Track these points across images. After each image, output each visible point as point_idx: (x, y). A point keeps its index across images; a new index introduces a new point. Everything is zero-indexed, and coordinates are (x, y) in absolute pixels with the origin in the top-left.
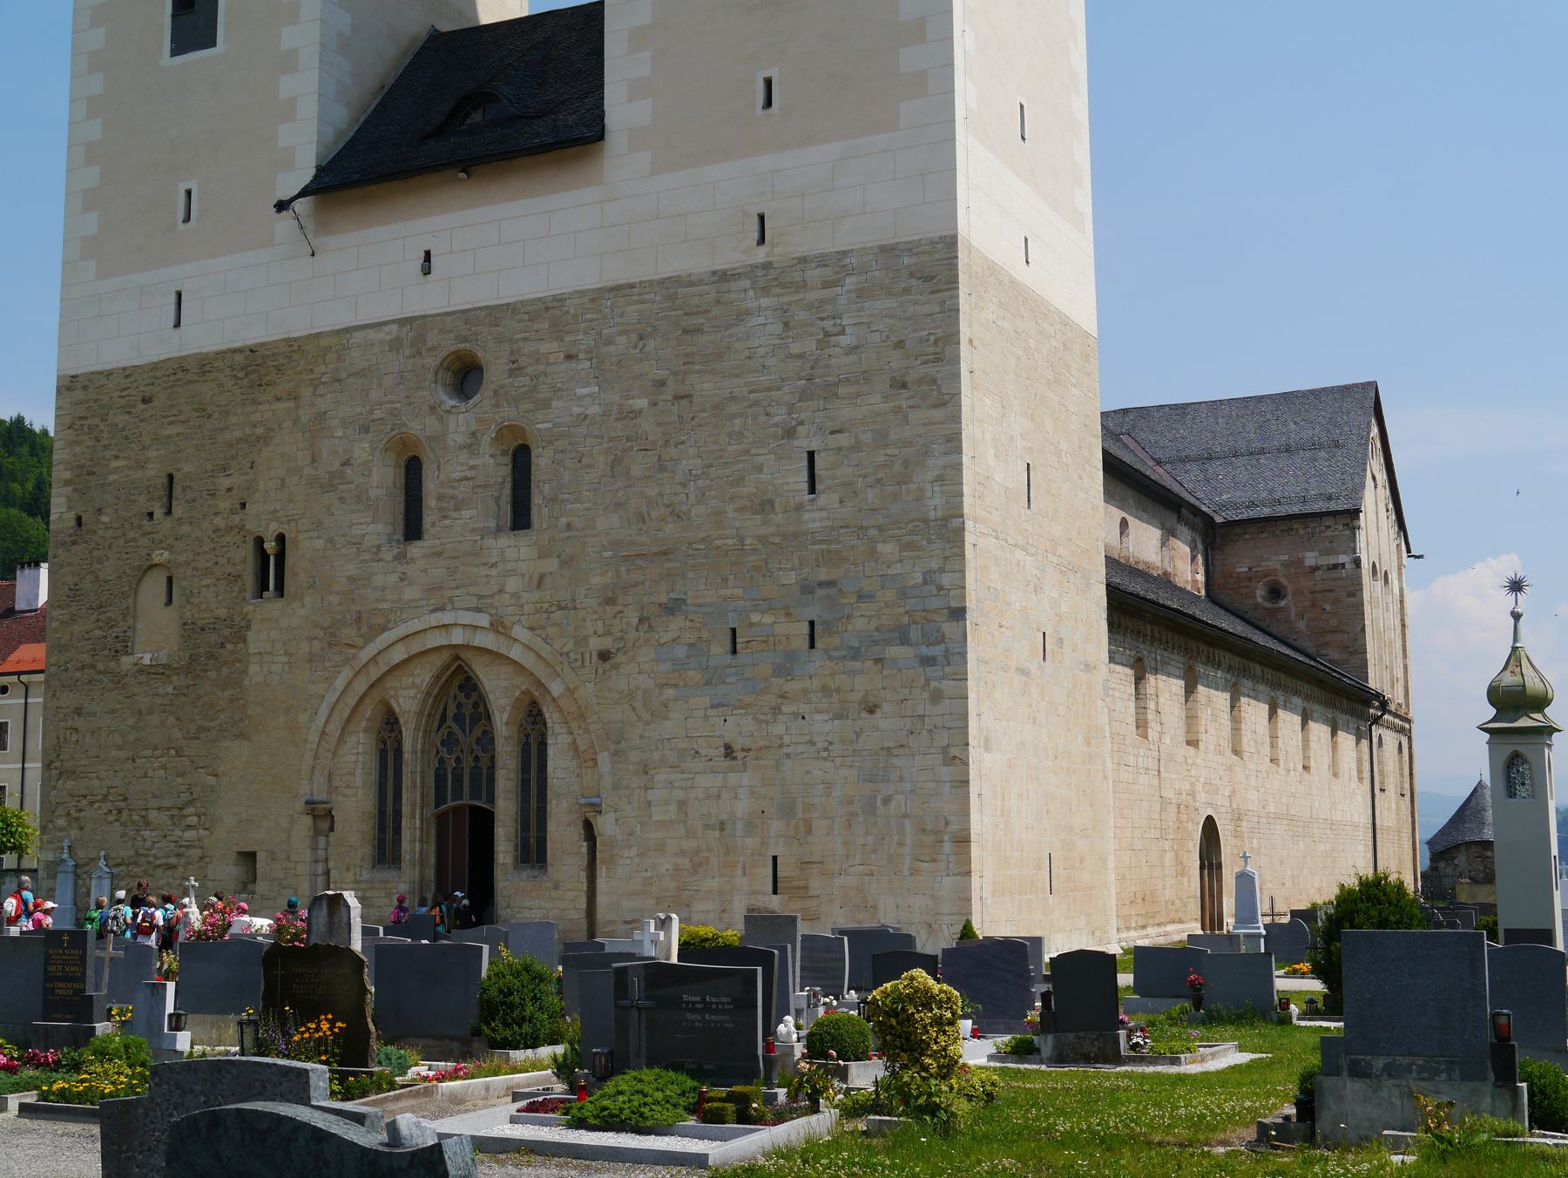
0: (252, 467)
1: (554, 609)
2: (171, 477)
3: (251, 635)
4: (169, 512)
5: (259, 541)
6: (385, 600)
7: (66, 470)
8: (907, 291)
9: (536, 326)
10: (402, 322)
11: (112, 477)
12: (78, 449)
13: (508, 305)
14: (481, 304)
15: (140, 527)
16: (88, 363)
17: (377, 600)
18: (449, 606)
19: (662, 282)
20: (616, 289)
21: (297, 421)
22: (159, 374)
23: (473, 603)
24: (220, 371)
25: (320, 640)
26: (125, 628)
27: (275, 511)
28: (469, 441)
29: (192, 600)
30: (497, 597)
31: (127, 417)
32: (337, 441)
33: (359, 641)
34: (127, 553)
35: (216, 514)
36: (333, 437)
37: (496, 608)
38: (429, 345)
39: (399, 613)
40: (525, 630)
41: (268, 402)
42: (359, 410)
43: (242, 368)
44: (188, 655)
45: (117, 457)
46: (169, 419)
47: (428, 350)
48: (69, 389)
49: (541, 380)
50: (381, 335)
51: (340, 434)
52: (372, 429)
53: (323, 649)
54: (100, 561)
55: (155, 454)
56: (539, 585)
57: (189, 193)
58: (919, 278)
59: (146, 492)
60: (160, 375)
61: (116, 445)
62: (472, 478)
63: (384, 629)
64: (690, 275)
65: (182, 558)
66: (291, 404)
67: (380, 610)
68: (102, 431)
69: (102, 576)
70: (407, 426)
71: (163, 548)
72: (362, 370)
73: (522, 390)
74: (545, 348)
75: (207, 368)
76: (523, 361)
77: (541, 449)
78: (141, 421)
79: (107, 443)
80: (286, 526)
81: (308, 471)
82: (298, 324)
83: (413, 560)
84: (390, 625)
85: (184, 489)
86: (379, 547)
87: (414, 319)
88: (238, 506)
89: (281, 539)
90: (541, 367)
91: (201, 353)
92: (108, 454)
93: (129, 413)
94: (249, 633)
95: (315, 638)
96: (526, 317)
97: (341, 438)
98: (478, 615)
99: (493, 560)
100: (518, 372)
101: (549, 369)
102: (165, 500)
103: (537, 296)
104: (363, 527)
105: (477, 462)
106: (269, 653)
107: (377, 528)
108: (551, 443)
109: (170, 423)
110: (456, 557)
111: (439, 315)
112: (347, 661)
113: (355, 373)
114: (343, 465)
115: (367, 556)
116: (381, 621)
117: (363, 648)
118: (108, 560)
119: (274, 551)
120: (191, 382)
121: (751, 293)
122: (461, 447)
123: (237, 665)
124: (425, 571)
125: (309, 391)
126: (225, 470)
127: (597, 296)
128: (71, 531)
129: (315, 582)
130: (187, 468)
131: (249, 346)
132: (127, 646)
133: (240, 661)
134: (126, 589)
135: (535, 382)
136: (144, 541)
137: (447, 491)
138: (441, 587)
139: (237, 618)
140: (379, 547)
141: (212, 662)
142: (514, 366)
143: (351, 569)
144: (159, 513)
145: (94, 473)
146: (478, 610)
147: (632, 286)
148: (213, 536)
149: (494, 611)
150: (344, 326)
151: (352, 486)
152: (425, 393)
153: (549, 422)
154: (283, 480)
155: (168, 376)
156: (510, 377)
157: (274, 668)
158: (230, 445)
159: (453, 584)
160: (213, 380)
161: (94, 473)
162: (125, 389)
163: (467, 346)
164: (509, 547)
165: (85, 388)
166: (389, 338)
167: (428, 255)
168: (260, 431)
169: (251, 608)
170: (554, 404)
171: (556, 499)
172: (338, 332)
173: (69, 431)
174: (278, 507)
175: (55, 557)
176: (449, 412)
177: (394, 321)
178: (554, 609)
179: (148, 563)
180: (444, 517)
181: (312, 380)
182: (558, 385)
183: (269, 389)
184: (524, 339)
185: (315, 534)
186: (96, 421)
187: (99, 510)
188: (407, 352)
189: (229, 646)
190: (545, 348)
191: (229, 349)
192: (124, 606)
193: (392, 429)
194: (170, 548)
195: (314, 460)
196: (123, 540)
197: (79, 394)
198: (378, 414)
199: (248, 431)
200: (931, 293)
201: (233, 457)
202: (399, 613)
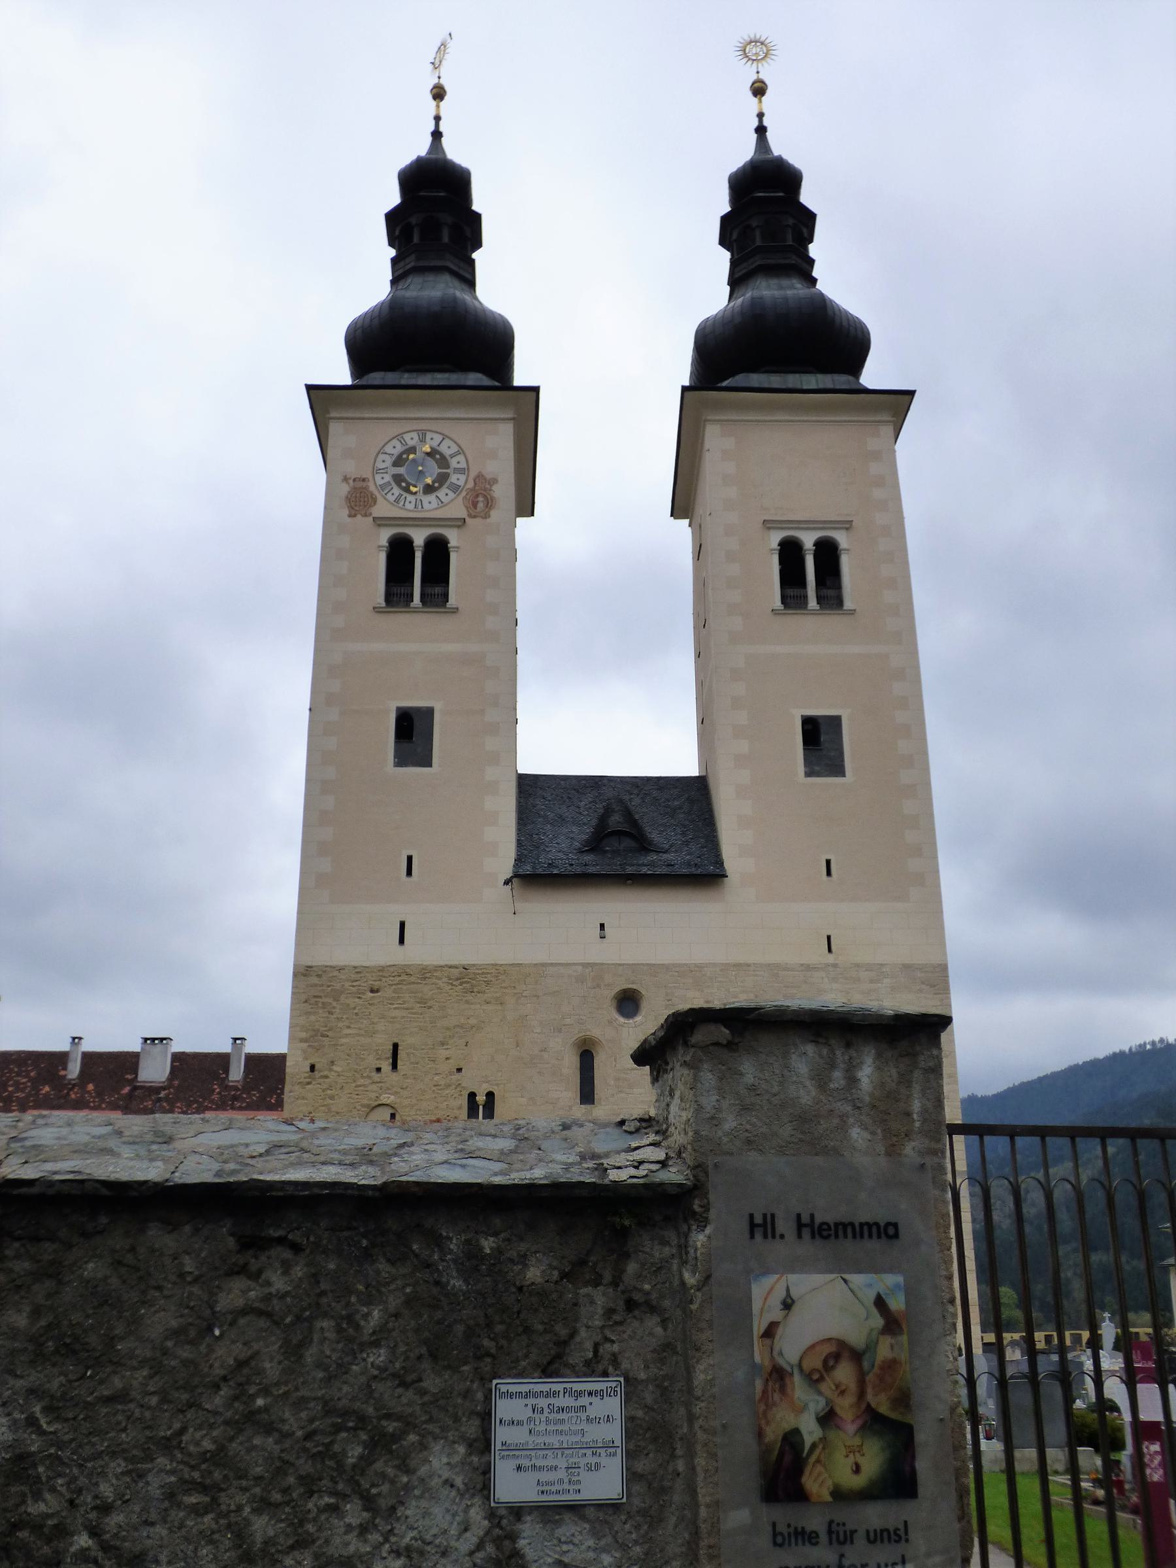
2: (396, 1046)
4: (395, 1066)
5: (472, 1096)
7: (301, 1031)
8: (921, 991)
10: (585, 965)
11: (343, 1041)
12: (313, 1018)
15: (369, 1077)
16: (322, 957)
19: (769, 965)
20: (738, 966)
22: (385, 974)
24: (440, 979)
31: (357, 1000)
41: (479, 1003)
43: (457, 979)
45: (349, 1027)
46: (394, 1006)
47: (605, 986)
48: (305, 975)
51: (538, 1030)
54: (332, 1098)
57: (410, 859)
58: (927, 985)
60: (387, 975)
61: (347, 1018)
64: (787, 964)
65: (406, 1102)
66: (499, 1007)
68: (334, 1008)
69: (334, 1109)
70: (589, 1031)
71: (389, 1094)
72: (555, 992)
75: (428, 975)
79: (340, 1016)
80: (496, 1087)
82: (504, 956)
85: (408, 1054)
86: (570, 1107)
87: (596, 964)
89: (490, 1095)
91: (422, 965)
92: (340, 1024)
93: (359, 998)
103: (685, 962)
107: (569, 1093)
109: (395, 1008)
111: (613, 964)
114: (542, 1051)
118: (340, 1098)
119: (483, 1103)
120: (413, 983)
121: (826, 980)
126: (443, 1044)
127: (725, 967)
128: (306, 1075)
131: (464, 965)
136: (374, 1087)
140: (570, 1107)
142: (667, 1003)
144: (386, 1066)
145: (328, 1036)
147: (748, 965)
148: (435, 1088)
150: (541, 962)
156: (666, 1009)
158: (448, 1029)
161: (328, 1036)
163: (634, 986)
165: (319, 976)
167: (602, 926)
168: (473, 1021)
173: (304, 1005)
175: (291, 1092)
176: (622, 1026)
179: (377, 1103)
181: (515, 994)
186: (329, 1000)
187: (332, 1062)
191: (446, 965)
194: (395, 1093)
195: (518, 1046)
197: (314, 980)
198: (568, 1021)
199: (462, 1021)
200: (935, 994)
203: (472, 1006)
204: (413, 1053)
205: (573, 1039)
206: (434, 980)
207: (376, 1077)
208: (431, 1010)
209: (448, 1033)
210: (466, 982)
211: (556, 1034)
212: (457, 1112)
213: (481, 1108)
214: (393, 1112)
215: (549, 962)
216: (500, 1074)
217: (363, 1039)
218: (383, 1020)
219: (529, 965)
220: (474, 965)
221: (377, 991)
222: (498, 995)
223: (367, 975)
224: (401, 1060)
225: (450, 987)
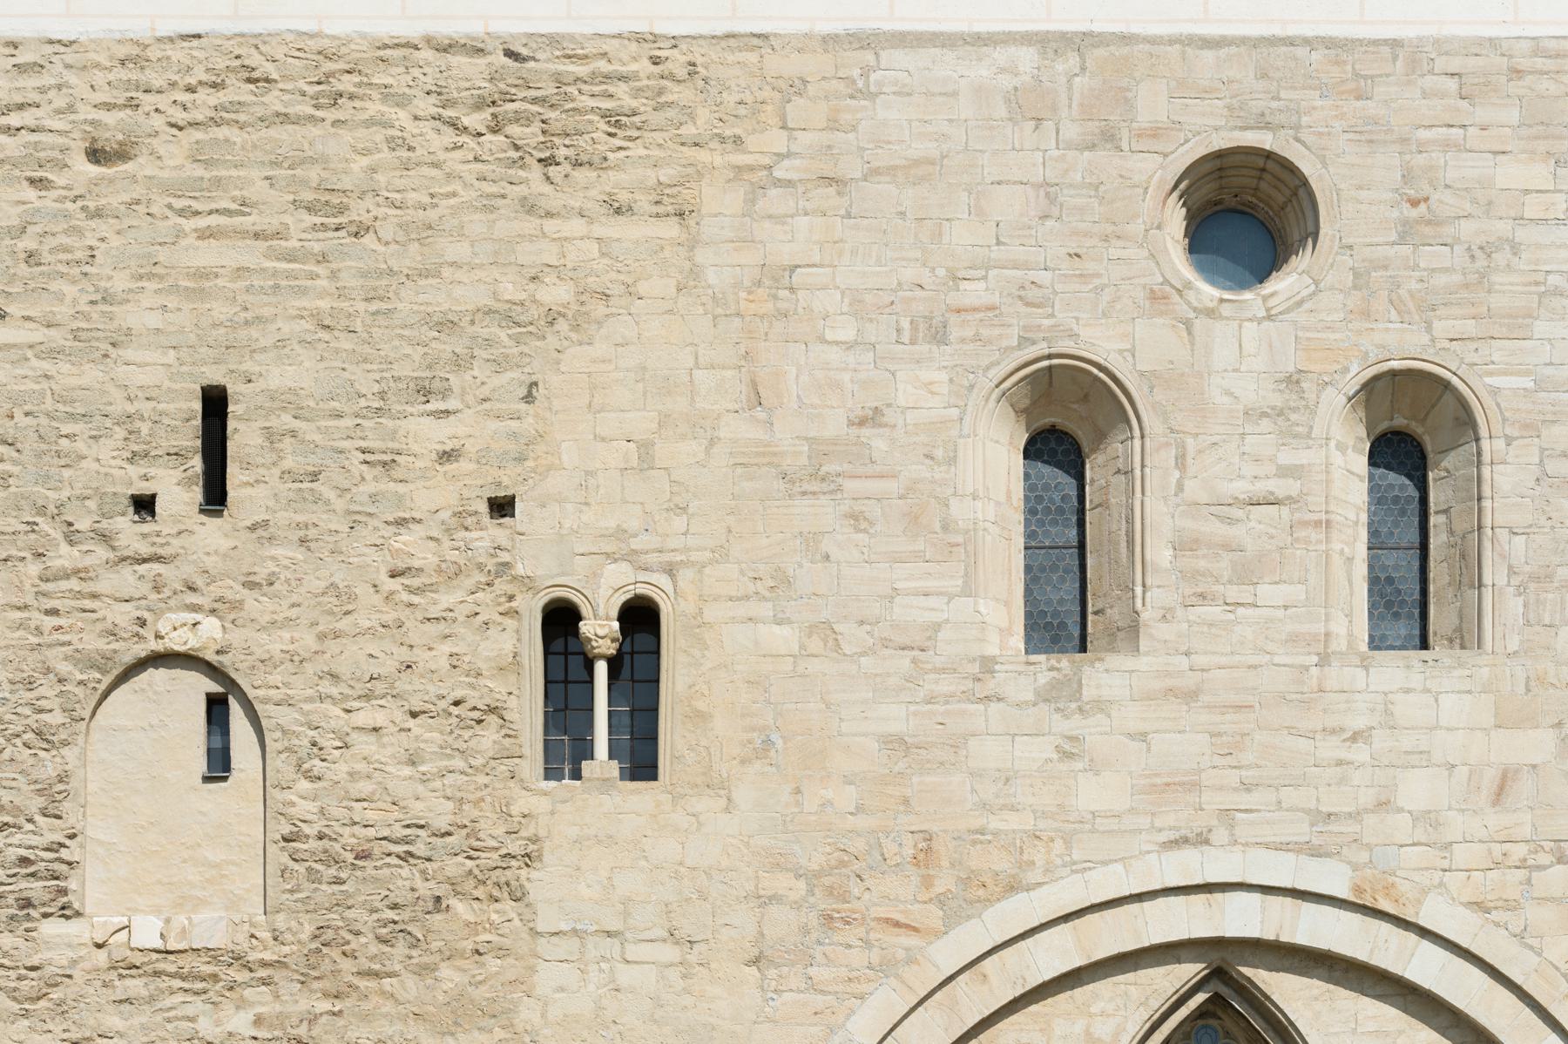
0: (529, 398)
1: (1544, 859)
2: (215, 404)
3: (541, 883)
4: (215, 495)
6: (1013, 809)
9: (1482, 114)
10: (1051, 43)
13: (1395, 44)
14: (1308, 32)
15: (105, 538)
17: (985, 806)
18: (1220, 835)
21: (689, 281)
23: (1300, 830)
24: (402, 101)
25: (797, 906)
26: (59, 837)
27: (621, 533)
28: (1277, 400)
29: (317, 766)
30: (1370, 820)
31: (31, 194)
32: (834, 355)
33: (933, 917)
34: (54, 612)
35: (401, 522)
36: (823, 340)
37: (1370, 848)
38: (1144, 118)
39: (1058, 846)
40: (1461, 908)
42: (909, 274)
43: (480, 104)
44: (309, 929)
46: (202, 222)
49: (1501, 258)
50: (983, 72)
51: (847, 333)
52: (955, 333)
53: (805, 931)
55: (154, 320)
56: (1499, 794)
59: (120, 433)
60: (157, 83)
62: (1290, 500)
63: (1013, 887)
65: (275, 643)
66: (670, 229)
67: (995, 834)
70: (1073, 336)
71: (195, 608)
72: (917, 163)
73: (1441, 280)
74: (1513, 174)
75: (346, 83)
76: (1445, 202)
77: (1500, 444)
78: (98, 214)
81: (740, 429)
83: (1101, 706)
84: (1033, 876)
85: (270, 435)
86: (988, 665)
88: (483, 508)
90: (1503, 228)
94: (534, 874)
95: (775, 898)
96: (1452, 84)
97: (849, 346)
98: (1314, 863)
99: (1360, 723)
100: (1427, 230)
101: (1522, 235)
102: (197, 463)
104: (932, 602)
105: (1303, 457)
106: (609, 934)
108: (1531, 429)
109: (205, 234)
110: (1239, 708)
111: (1172, 41)
112: (885, 968)
113: (891, 170)
114: (862, 422)
115: (946, 685)
116: (1001, 862)
117: (938, 934)
119: (610, 648)
120: (284, 118)
122: (1252, 414)
123: (493, 964)
124: (1143, 737)
125: (734, 200)
126: (425, 393)
129: (768, 742)
130: (278, 377)
132: (63, 892)
133: (502, 952)
134: (56, 718)
135: (1481, 262)
136: (127, 580)
137: (1214, 529)
138: (1194, 786)
139: (492, 829)
141: (401, 949)
142: (1414, 213)
143: (895, 717)
146: (1317, 852)
148: (395, 584)
149: (1364, 856)
151: (892, 486)
152: (1133, 252)
153: (1527, 373)
154: (645, 447)
155: (190, 89)
156: (1402, 240)
157: (625, 975)
158: (446, 325)
159: (1233, 777)
160: (370, 123)
162: (21, 107)
163: (1264, 140)
164: (1408, 691)
166: (1006, 82)
168: (556, 293)
169: (540, 805)
170: (1541, 328)
171: (1549, 577)
172: (830, 41)
174: (634, 524)
176: (1210, 313)
177: (1027, 39)
178: (1544, 859)
179: (141, 650)
180: (1202, 596)
181: (739, 169)
182: (1553, 280)
183: (582, 175)
184: (1447, 145)
185: (766, 610)
188: (1071, 131)
189: (459, 907)
190: (1513, 174)
191: (429, 40)
192: (50, 770)
193: (1024, 341)
196: (34, 569)
198: (974, 292)
199: (510, 290)
201: (460, 363)
202: (1058, 846)
203: (550, 225)
204: (293, 433)
205: (997, 373)
206: (374, 108)
207: (127, 527)
208: (368, 240)
209: (448, 346)
210: (519, 118)
211: (923, 348)
212: (497, 688)
213: (601, 669)
214: (216, 688)
215: (887, 26)
216: (679, 523)
217: (65, 367)
218: (151, 285)
219: (804, 43)
220: (553, 40)
221: (121, 154)
222: (666, 174)
223: (71, 77)
224: (247, 466)
225: (449, 136)
